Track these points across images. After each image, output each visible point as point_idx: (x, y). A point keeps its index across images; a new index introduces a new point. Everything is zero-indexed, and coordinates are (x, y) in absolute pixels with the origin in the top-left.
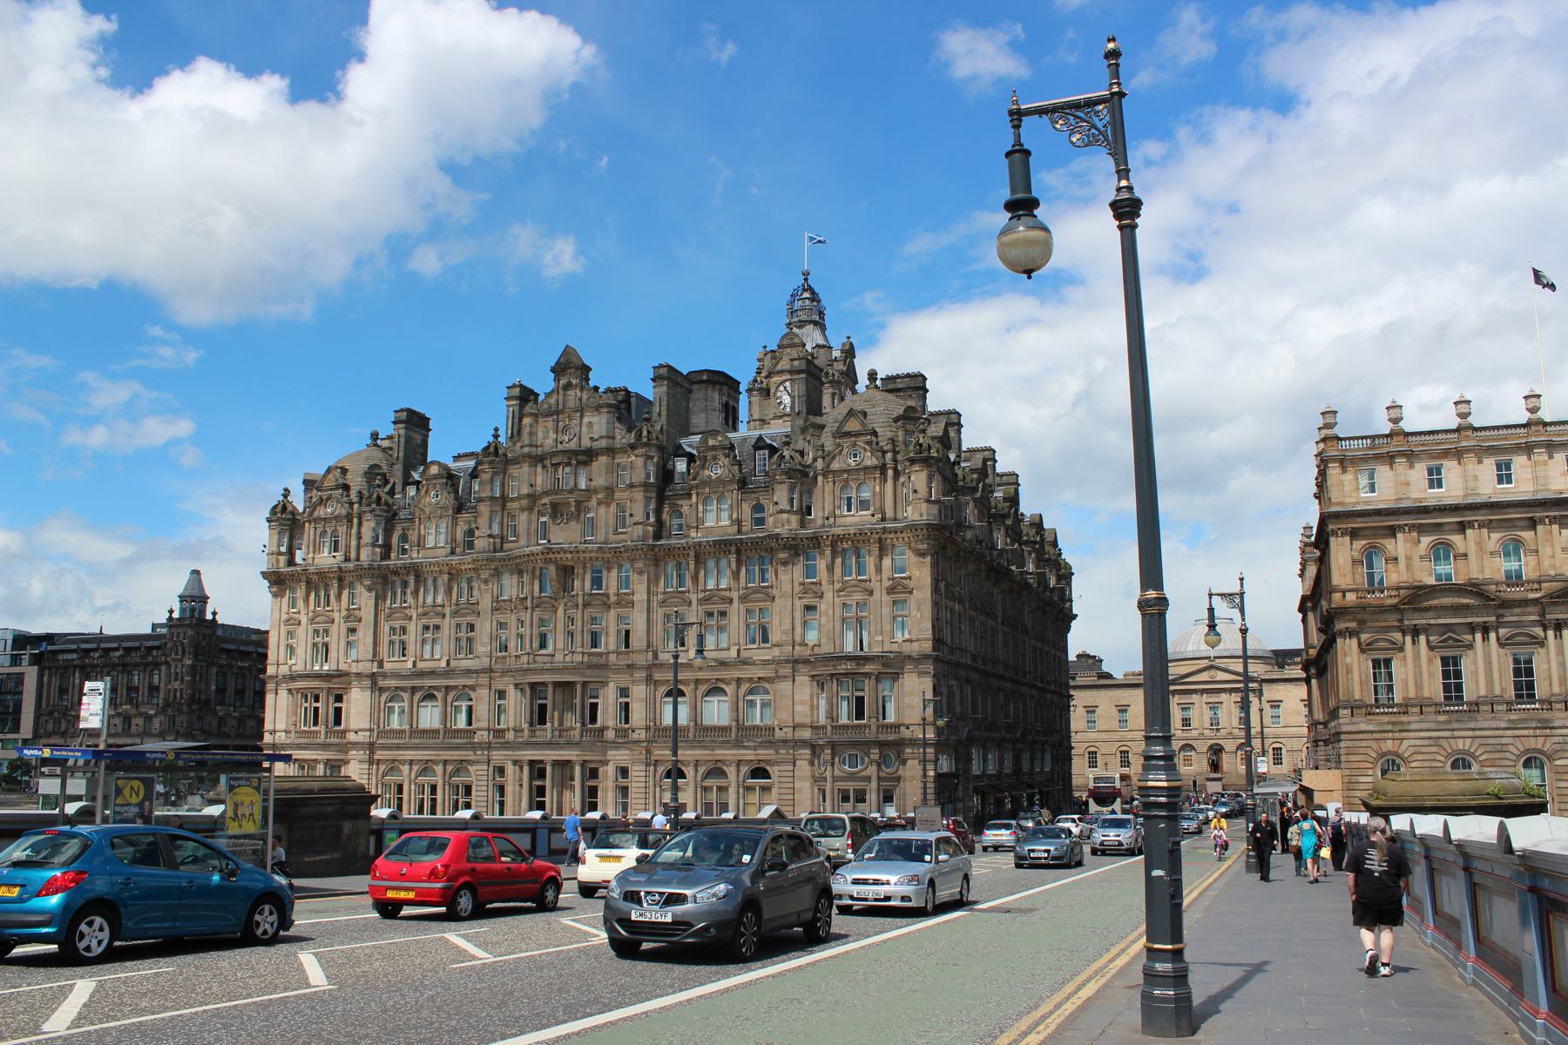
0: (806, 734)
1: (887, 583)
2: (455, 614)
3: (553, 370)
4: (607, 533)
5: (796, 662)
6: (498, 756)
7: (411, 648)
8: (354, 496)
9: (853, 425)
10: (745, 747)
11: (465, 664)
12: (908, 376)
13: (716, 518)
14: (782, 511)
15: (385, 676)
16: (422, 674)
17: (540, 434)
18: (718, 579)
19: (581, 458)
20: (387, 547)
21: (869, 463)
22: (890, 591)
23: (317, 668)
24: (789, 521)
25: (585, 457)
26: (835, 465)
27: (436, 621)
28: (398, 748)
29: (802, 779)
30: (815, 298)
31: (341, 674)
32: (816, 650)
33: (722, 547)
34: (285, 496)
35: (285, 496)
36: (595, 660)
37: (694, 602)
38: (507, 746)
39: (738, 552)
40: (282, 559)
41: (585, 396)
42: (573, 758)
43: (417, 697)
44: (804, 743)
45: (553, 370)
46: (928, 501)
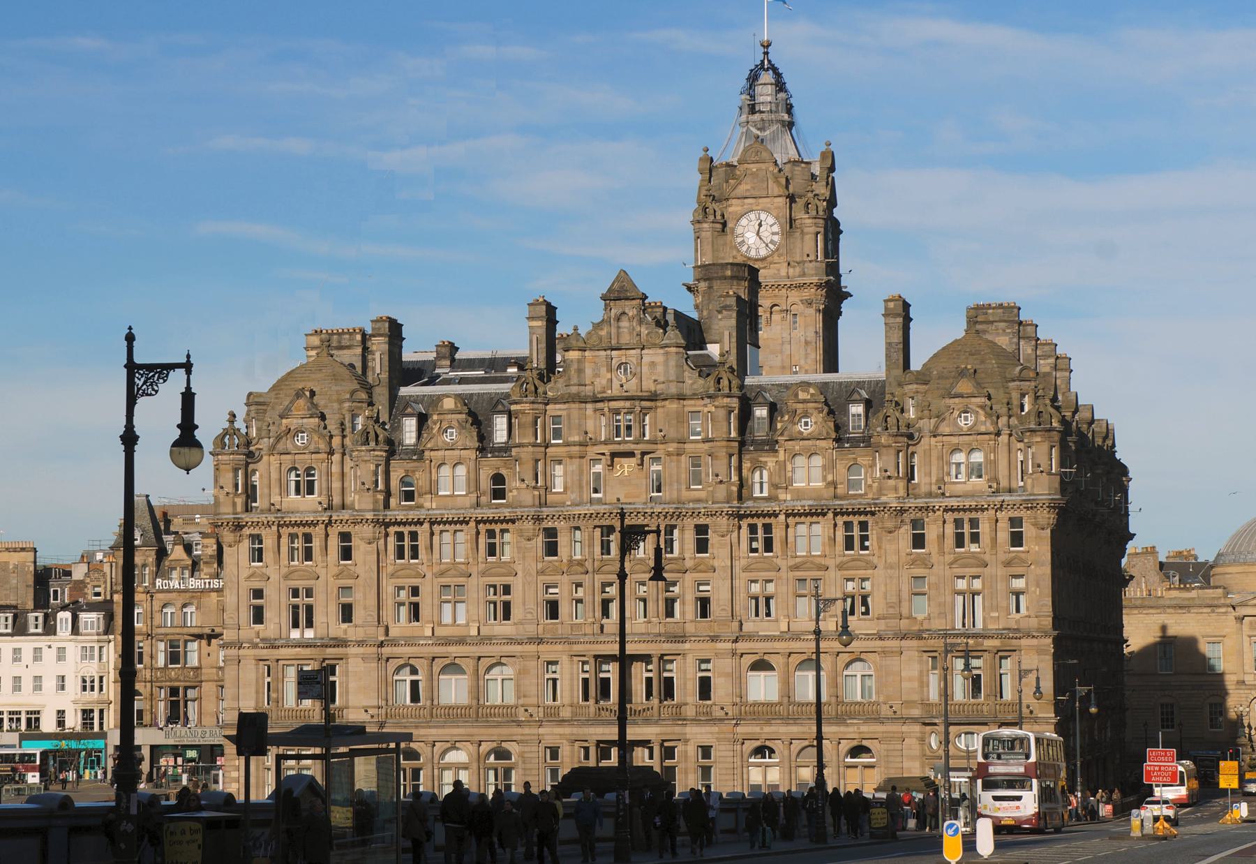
0: (916, 712)
1: (1002, 557)
2: (483, 574)
3: (604, 298)
4: (679, 490)
7: (424, 611)
8: (333, 426)
10: (847, 725)
14: (889, 477)
15: (394, 643)
16: (447, 642)
17: (588, 371)
19: (645, 404)
21: (983, 429)
24: (896, 489)
27: (462, 580)
29: (912, 758)
30: (780, 86)
31: (340, 643)
32: (925, 626)
34: (231, 422)
35: (231, 422)
37: (784, 568)
38: (562, 722)
40: (240, 501)
41: (644, 331)
44: (914, 720)
45: (604, 298)
46: (1050, 474)
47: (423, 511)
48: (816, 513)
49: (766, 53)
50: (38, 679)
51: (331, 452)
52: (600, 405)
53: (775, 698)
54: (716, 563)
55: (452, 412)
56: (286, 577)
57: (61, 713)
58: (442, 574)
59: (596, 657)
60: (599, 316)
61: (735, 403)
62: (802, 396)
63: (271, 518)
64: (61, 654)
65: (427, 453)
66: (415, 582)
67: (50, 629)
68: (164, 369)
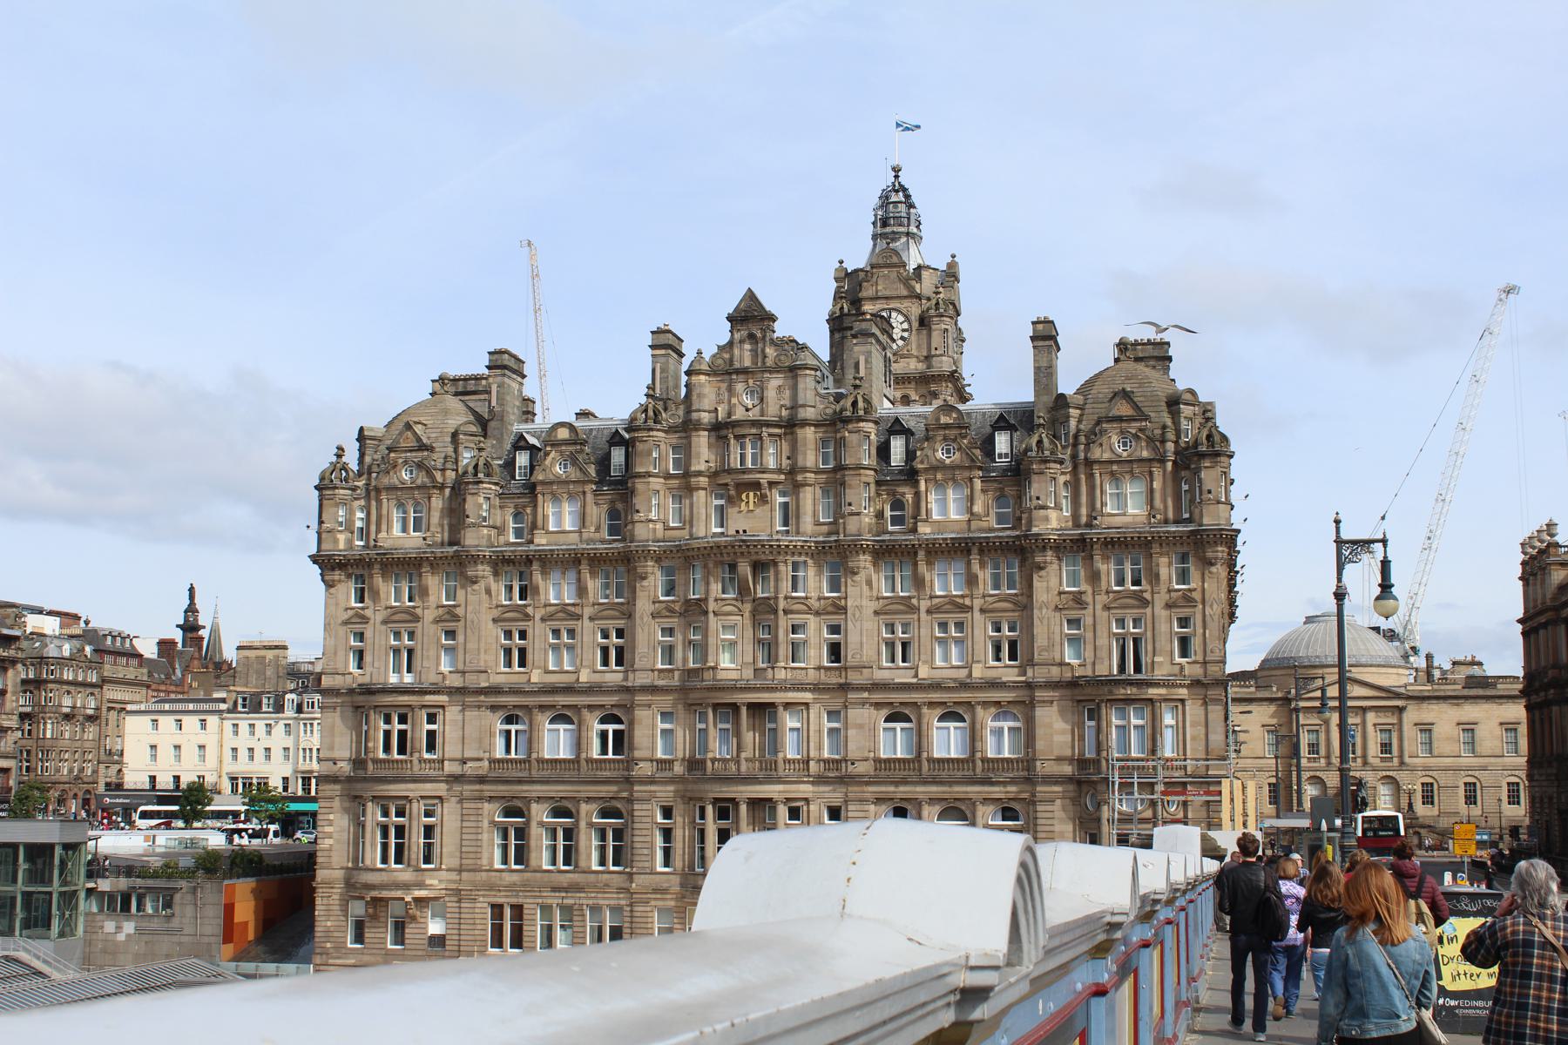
0: (1068, 769)
3: (730, 318)
9: (1123, 409)
12: (1149, 342)
13: (945, 510)
23: (393, 679)
24: (1047, 519)
26: (1106, 456)
28: (520, 782)
33: (959, 549)
34: (339, 456)
35: (339, 456)
36: (800, 676)
37: (923, 609)
39: (981, 552)
42: (775, 796)
45: (730, 318)
47: (532, 547)
49: (897, 177)
50: (268, 750)
52: (724, 432)
55: (565, 442)
59: (716, 706)
60: (725, 338)
62: (944, 420)
65: (539, 488)
66: (522, 625)
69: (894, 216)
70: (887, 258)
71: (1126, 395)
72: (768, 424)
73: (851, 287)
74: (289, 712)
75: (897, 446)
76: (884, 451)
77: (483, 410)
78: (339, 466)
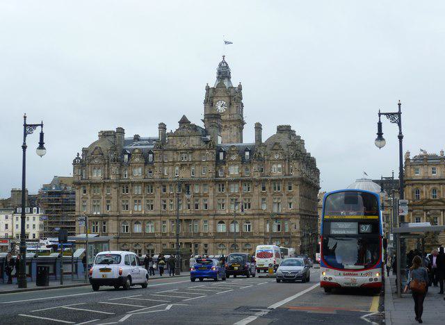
0: (263, 235)
5: (260, 215)
6: (164, 241)
7: (130, 207)
9: (276, 147)
11: (150, 212)
13: (234, 171)
18: (234, 189)
20: (120, 175)
22: (287, 195)
25: (192, 150)
26: (271, 158)
27: (140, 199)
33: (236, 181)
36: (197, 213)
38: (167, 238)
43: (133, 223)
44: (263, 237)
48: (236, 181)
51: (105, 164)
53: (225, 231)
54: (210, 195)
56: (93, 198)
57: (34, 235)
58: (134, 197)
61: (214, 151)
63: (88, 181)
64: (34, 219)
67: (31, 212)
68: (35, 126)
69: (224, 73)
70: (220, 85)
71: (276, 144)
72: (189, 150)
73: (211, 96)
74: (35, 213)
75: (221, 155)
76: (218, 156)
77: (111, 140)
78: (78, 158)
